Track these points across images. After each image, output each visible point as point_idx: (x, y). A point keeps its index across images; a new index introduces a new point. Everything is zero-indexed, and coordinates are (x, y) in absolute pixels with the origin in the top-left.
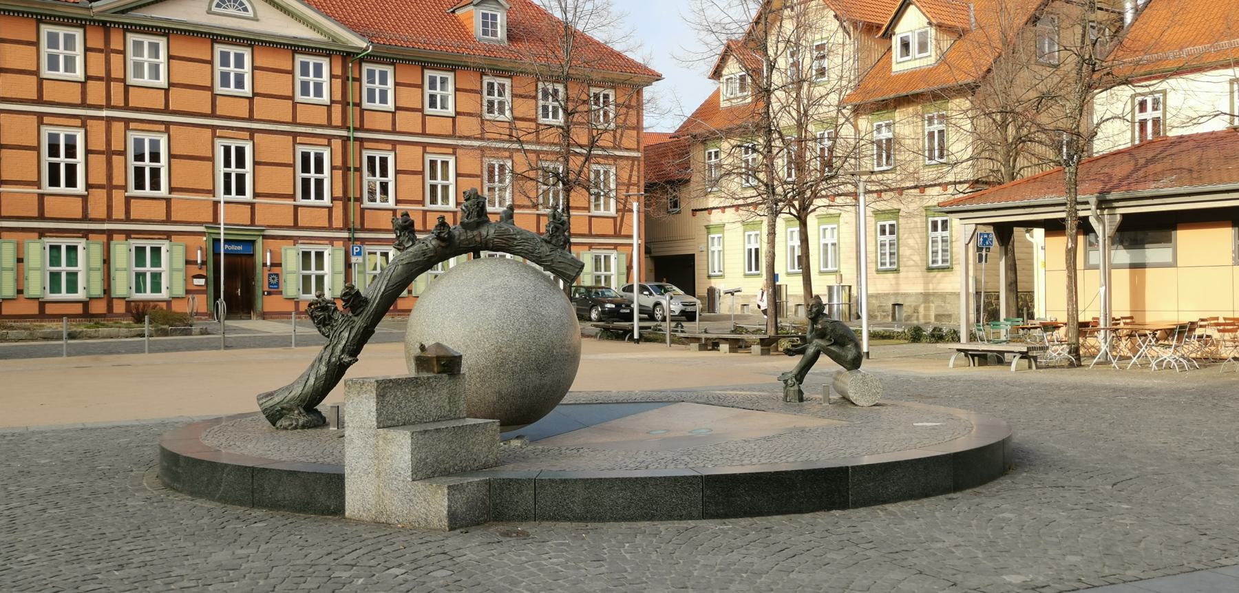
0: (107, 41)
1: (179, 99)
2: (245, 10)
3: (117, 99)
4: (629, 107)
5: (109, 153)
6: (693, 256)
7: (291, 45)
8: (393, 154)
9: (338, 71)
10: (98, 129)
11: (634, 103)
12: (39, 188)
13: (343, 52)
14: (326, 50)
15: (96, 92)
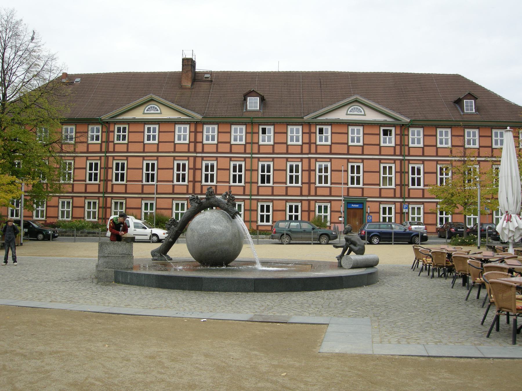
0: (310, 130)
1: (336, 149)
3: (313, 150)
5: (310, 170)
8: (422, 165)
9: (398, 132)
10: (306, 161)
12: (286, 184)
13: (401, 124)
14: (393, 124)
15: (306, 148)
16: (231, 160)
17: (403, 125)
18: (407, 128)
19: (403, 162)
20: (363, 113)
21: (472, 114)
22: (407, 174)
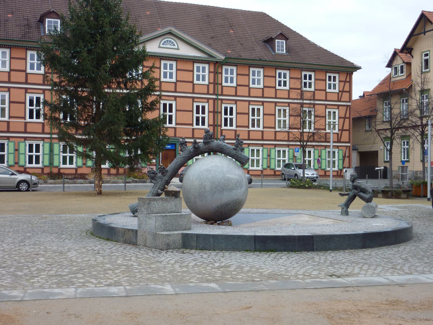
2: (174, 45)
4: (345, 82)
6: (378, 151)
7: (193, 60)
9: (212, 70)
11: (348, 80)
13: (215, 61)
14: (207, 61)
16: (26, 92)
17: (217, 62)
18: (221, 66)
19: (216, 101)
20: (176, 47)
21: (282, 55)
22: (219, 115)
